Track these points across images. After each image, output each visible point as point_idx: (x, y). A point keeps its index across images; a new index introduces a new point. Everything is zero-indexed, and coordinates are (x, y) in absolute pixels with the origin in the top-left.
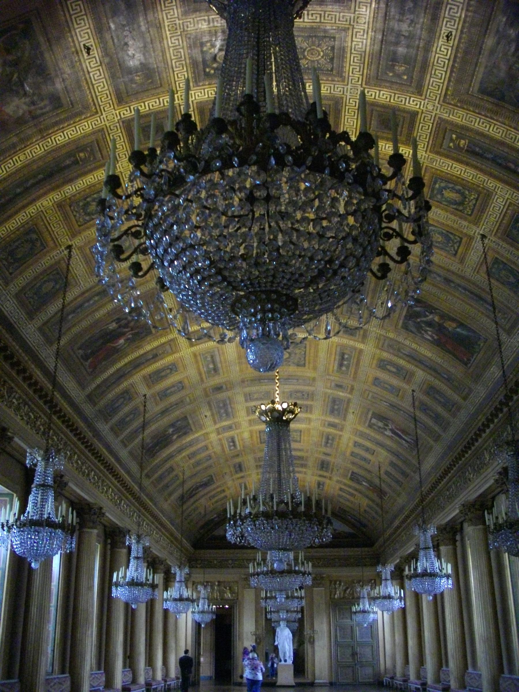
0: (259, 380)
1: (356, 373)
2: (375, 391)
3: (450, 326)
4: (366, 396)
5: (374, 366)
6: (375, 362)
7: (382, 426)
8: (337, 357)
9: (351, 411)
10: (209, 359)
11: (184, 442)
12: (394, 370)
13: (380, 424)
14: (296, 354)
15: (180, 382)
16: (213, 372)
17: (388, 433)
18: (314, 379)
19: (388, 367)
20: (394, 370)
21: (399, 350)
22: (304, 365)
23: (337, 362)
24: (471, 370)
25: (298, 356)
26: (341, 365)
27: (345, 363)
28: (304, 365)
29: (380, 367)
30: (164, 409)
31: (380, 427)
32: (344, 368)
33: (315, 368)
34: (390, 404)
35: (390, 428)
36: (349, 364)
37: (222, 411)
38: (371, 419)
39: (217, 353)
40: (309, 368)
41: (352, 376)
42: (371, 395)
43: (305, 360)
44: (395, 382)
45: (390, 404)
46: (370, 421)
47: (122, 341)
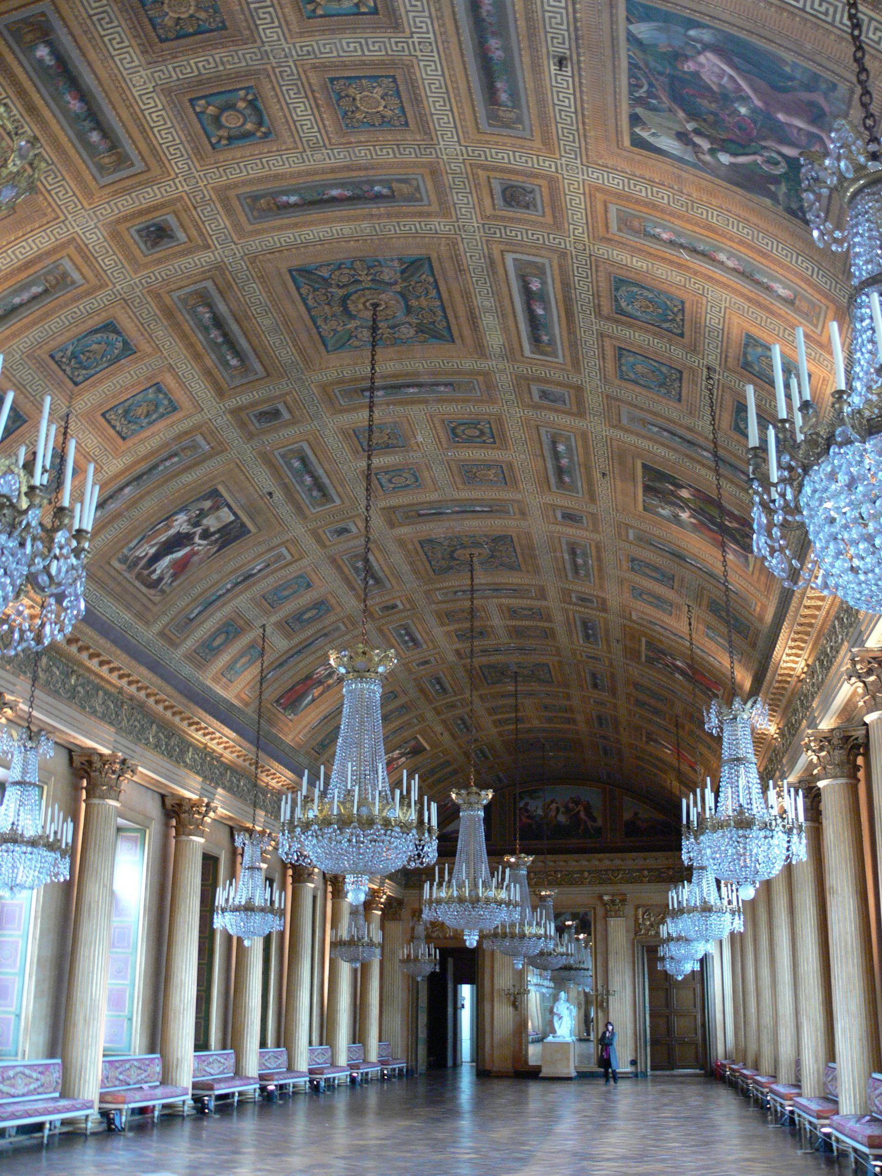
0: (491, 511)
1: (339, 568)
2: (291, 568)
3: (316, 692)
4: (293, 550)
5: (330, 597)
6: (333, 601)
7: (205, 522)
8: (381, 574)
9: (279, 495)
10: (582, 572)
11: (672, 456)
12: (306, 617)
13: (212, 523)
14: (443, 559)
15: (633, 569)
16: (578, 551)
17: (180, 523)
18: (392, 525)
19: (314, 612)
20: (306, 617)
21: (325, 635)
23: (375, 564)
24: (269, 706)
25: (439, 555)
29: (322, 603)
30: (677, 560)
31: (202, 514)
32: (360, 564)
33: (402, 543)
34: (252, 575)
35: (197, 539)
37: (564, 461)
39: (570, 575)
40: (412, 541)
41: (340, 562)
42: (289, 557)
43: (426, 554)
44: (289, 608)
45: (252, 575)
47: (678, 663)
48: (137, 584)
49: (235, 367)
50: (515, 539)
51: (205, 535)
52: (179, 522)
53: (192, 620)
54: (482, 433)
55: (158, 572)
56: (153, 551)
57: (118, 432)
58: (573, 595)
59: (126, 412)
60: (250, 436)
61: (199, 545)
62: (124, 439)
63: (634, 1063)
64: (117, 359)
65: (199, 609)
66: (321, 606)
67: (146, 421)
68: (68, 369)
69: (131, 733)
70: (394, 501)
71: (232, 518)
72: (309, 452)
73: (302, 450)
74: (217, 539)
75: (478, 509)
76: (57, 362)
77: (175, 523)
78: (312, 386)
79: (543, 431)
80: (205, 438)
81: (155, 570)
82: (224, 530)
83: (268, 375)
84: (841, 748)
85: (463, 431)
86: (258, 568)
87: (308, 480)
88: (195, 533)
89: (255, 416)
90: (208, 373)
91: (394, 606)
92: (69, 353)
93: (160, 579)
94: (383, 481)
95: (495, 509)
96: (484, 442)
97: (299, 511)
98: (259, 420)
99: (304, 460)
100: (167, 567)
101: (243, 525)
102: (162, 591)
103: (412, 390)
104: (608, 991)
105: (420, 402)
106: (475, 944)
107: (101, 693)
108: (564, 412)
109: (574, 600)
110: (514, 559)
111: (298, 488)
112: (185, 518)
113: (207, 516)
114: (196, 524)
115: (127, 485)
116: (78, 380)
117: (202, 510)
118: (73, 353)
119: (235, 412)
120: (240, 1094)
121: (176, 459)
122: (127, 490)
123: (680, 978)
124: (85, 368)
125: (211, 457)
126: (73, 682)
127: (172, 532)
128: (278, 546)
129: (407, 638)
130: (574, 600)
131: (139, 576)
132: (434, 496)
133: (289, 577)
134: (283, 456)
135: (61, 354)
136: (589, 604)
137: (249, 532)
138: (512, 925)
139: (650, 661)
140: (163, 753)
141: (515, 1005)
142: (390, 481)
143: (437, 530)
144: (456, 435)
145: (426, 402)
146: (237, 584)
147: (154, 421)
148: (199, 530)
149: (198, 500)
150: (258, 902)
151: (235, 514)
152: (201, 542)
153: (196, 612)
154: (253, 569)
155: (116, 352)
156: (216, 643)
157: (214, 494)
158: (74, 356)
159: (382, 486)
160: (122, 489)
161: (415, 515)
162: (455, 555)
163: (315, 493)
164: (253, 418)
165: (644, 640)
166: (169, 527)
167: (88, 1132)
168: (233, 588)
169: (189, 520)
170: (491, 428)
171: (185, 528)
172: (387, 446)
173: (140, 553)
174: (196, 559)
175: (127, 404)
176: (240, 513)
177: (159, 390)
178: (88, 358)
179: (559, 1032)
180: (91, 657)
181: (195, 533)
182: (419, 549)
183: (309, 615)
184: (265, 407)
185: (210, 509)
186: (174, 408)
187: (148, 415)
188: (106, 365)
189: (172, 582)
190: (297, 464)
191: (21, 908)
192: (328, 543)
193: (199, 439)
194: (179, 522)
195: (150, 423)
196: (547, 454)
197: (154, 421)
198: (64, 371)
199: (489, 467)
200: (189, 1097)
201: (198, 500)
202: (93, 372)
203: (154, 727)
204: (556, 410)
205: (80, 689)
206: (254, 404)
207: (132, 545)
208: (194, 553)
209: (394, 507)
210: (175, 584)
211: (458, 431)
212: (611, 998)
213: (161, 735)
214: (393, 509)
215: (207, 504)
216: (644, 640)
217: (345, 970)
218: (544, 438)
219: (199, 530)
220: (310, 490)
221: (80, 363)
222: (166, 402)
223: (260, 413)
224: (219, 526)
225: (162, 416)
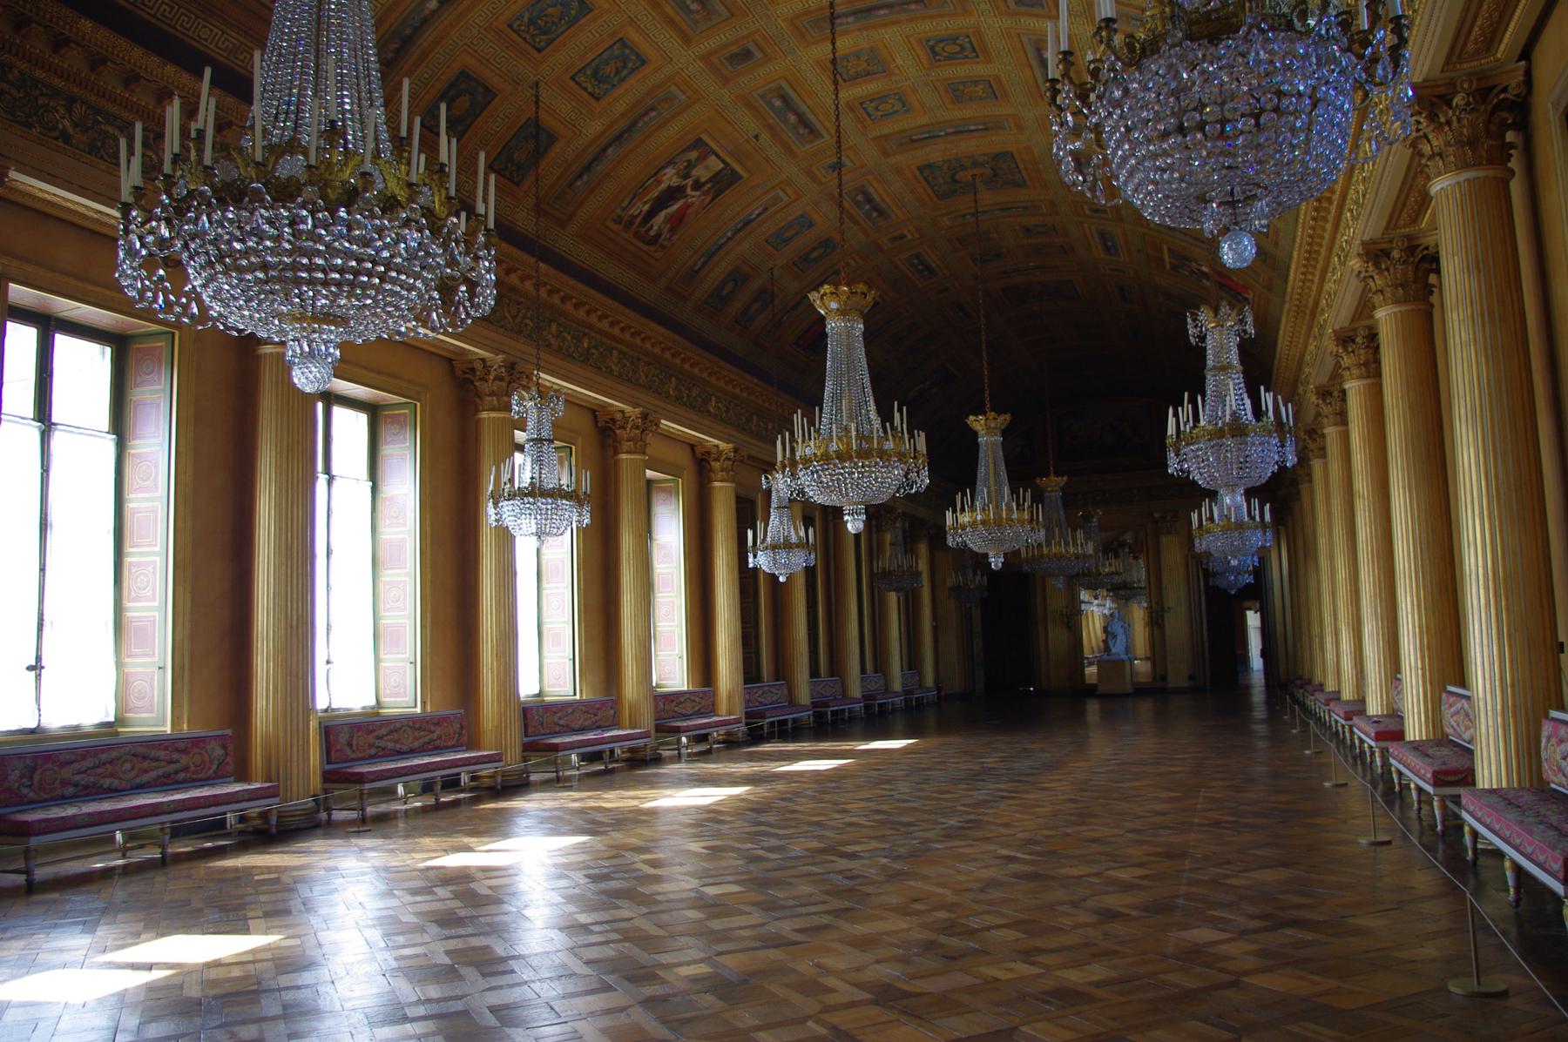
7: (694, 172)
8: (884, 206)
9: (765, 138)
13: (701, 173)
16: (1083, 160)
17: (670, 177)
18: (886, 154)
19: (821, 250)
22: (921, 169)
23: (875, 196)
26: (869, 199)
27: (867, 207)
28: (919, 168)
29: (827, 240)
31: (690, 165)
32: (860, 198)
34: (750, 222)
35: (689, 191)
36: (861, 209)
38: (723, 161)
42: (786, 198)
43: (925, 178)
45: (750, 222)
46: (718, 156)
47: (1204, 269)
48: (636, 242)
49: (697, 11)
50: (1016, 155)
51: (697, 185)
52: (668, 176)
53: (697, 272)
54: (962, 48)
55: (655, 228)
56: (646, 208)
57: (590, 93)
58: (1086, 207)
59: (595, 72)
60: (725, 80)
61: (693, 197)
62: (598, 99)
63: (1191, 677)
64: (576, 19)
65: (702, 260)
66: (826, 244)
67: (616, 79)
68: (528, 37)
69: (650, 388)
70: (886, 129)
71: (722, 166)
72: (788, 90)
73: (781, 88)
74: (710, 189)
75: (972, 128)
76: (515, 31)
77: (665, 178)
78: (779, 20)
79: (1024, 39)
80: (680, 89)
81: (652, 227)
82: (714, 179)
83: (732, 15)
84: (1367, 347)
85: (943, 48)
86: (757, 212)
87: (792, 118)
88: (686, 185)
89: (726, 59)
90: (670, 22)
91: (903, 237)
92: (526, 20)
93: (659, 235)
94: (869, 109)
95: (990, 126)
96: (966, 57)
97: (789, 150)
98: (731, 63)
99: (784, 98)
100: (663, 222)
101: (733, 171)
102: (664, 247)
103: (882, 12)
104: (1163, 608)
105: (893, 23)
106: (1000, 565)
107: (615, 352)
108: (1043, 16)
109: (1087, 212)
110: (1018, 176)
111: (783, 126)
112: (674, 171)
113: (695, 166)
114: (686, 176)
115: (610, 145)
116: (537, 46)
117: (689, 161)
118: (530, 20)
119: (706, 58)
120: (794, 720)
121: (653, 114)
122: (610, 151)
123: (1233, 592)
124: (545, 33)
125: (689, 106)
126: (586, 345)
127: (663, 186)
128: (773, 188)
129: (920, 267)
130: (1087, 212)
131: (636, 234)
132: (924, 120)
133: (790, 218)
134: (762, 97)
135: (518, 23)
136: (1102, 215)
137: (741, 177)
138: (1040, 545)
139: (1174, 268)
140: (685, 404)
141: (1069, 627)
142: (877, 109)
143: (936, 153)
144: (935, 54)
145: (899, 22)
146: (739, 230)
147: (625, 77)
148: (689, 182)
149: (683, 151)
150: (794, 539)
151: (723, 161)
152: (694, 193)
153: (700, 263)
154: (750, 215)
155: (573, 12)
156: (725, 292)
157: (699, 143)
158: (532, 22)
159: (869, 115)
160: (605, 150)
161: (910, 141)
162: (957, 177)
163: (801, 131)
164: (725, 61)
165: (1165, 248)
166: (659, 182)
167: (648, 758)
168: (733, 235)
169: (678, 173)
170: (971, 42)
171: (675, 182)
172: (868, 74)
173: (633, 211)
174: (691, 210)
175: (594, 64)
176: (728, 160)
177: (625, 45)
178: (547, 22)
179: (1113, 650)
180: (600, 318)
181: (686, 185)
182: (919, 176)
183: (815, 254)
184: (735, 49)
185: (698, 159)
186: (642, 61)
187: (618, 72)
188: (564, 28)
189: (671, 236)
190: (778, 103)
191: (563, 561)
192: (823, 180)
193: (674, 89)
194: (668, 176)
195: (622, 80)
196: (1034, 63)
197: (625, 77)
198: (525, 39)
199: (976, 83)
200: (743, 724)
201: (683, 151)
202: (554, 36)
203: (673, 380)
204: (1037, 16)
205: (593, 351)
206: (723, 47)
207: (624, 205)
208: (688, 206)
209: (885, 136)
210: (674, 238)
211: (937, 49)
212: (1166, 615)
213: (681, 387)
214: (885, 137)
215: (694, 155)
216: (1165, 248)
217: (893, 598)
218: (1028, 46)
219: (689, 182)
220: (795, 128)
221: (540, 28)
222: (634, 57)
223: (731, 56)
224: (711, 175)
225: (632, 72)
